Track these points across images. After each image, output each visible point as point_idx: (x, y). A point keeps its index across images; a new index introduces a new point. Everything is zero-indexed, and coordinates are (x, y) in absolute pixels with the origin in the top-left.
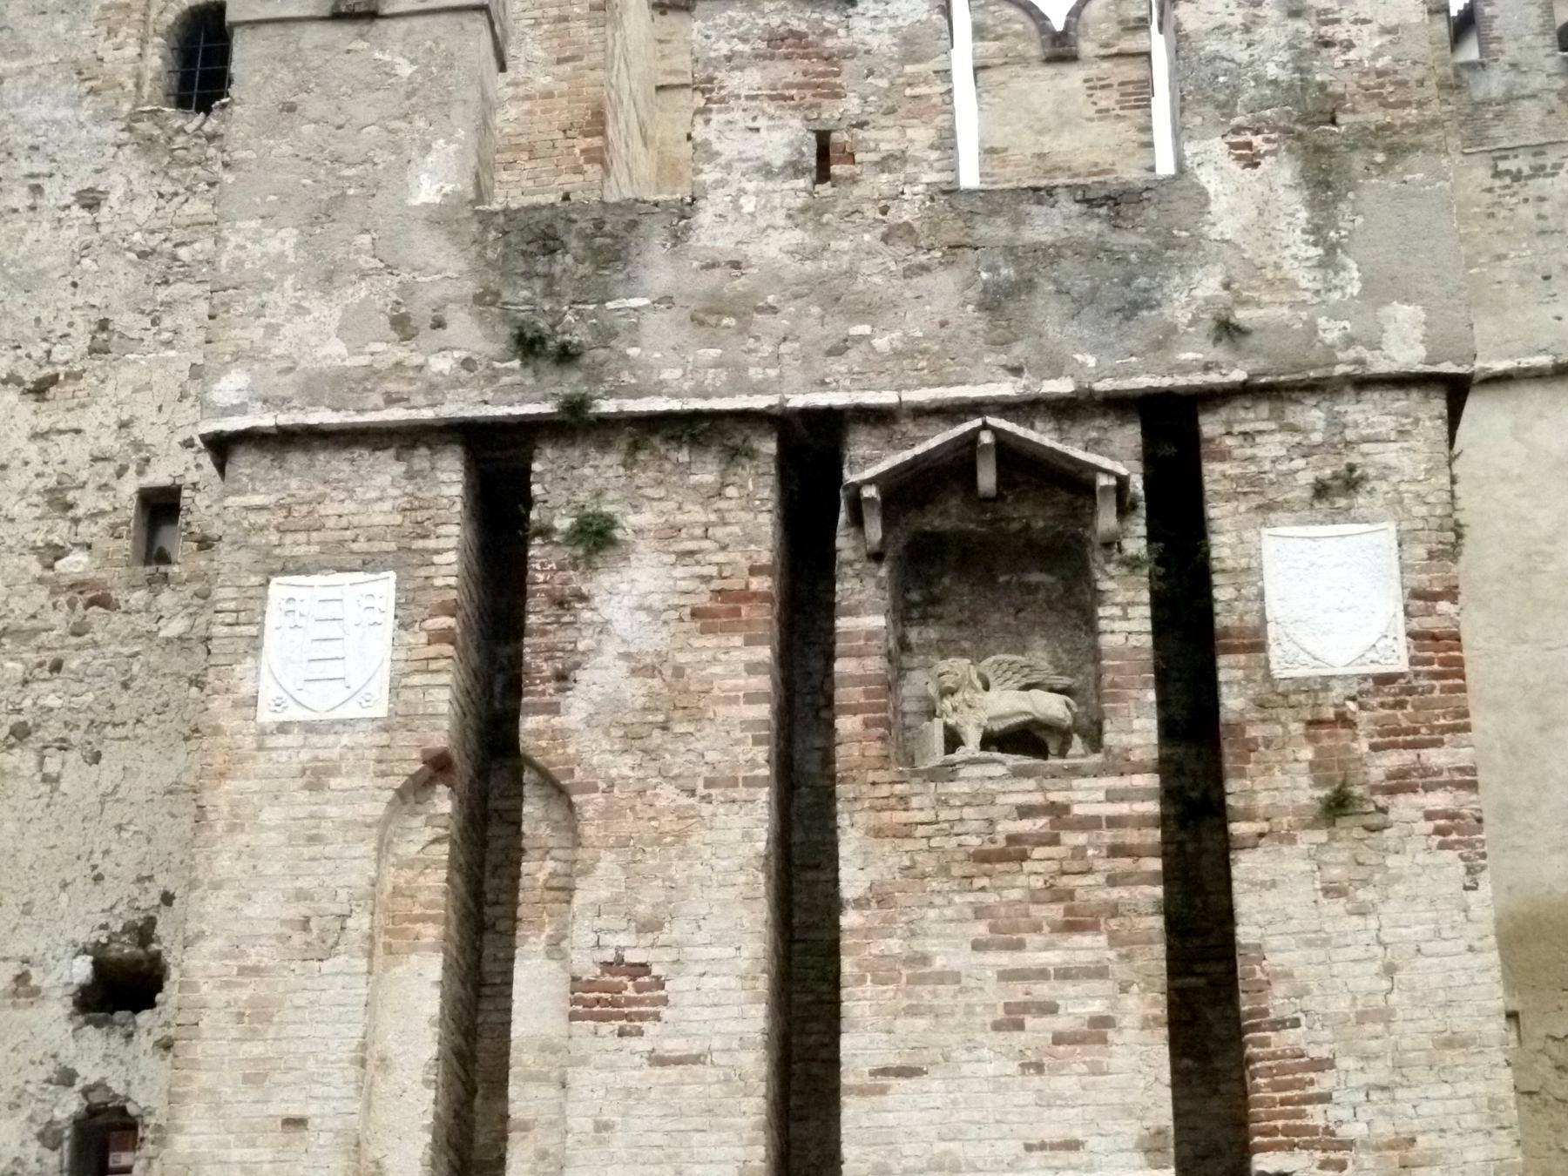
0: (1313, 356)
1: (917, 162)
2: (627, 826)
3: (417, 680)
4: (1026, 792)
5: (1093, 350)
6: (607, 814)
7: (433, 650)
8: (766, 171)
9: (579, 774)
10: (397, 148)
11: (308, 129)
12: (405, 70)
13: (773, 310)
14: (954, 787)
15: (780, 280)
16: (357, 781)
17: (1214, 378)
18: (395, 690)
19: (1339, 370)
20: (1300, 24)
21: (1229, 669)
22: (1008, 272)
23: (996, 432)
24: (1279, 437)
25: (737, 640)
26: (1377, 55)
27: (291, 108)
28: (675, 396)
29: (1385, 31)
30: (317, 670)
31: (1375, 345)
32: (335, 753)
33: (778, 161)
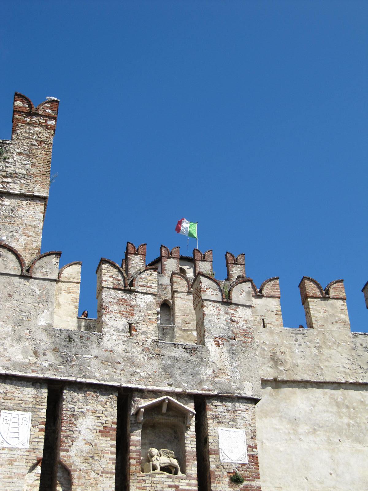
0: (231, 391)
1: (150, 333)
2: (83, 481)
3: (36, 440)
4: (170, 482)
5: (187, 382)
6: (79, 478)
7: (40, 433)
8: (118, 330)
9: (73, 467)
10: (36, 310)
11: (14, 302)
12: (38, 292)
13: (119, 363)
14: (154, 479)
15: (121, 356)
16: (21, 464)
17: (211, 393)
18: (32, 442)
19: (235, 395)
20: (227, 316)
21: (212, 458)
22: (169, 362)
23: (169, 400)
24: (222, 407)
25: (109, 439)
26: (243, 326)
27: (11, 296)
28: (98, 380)
29: (245, 320)
30: (12, 435)
31: (242, 390)
32: (16, 456)
33: (121, 328)
